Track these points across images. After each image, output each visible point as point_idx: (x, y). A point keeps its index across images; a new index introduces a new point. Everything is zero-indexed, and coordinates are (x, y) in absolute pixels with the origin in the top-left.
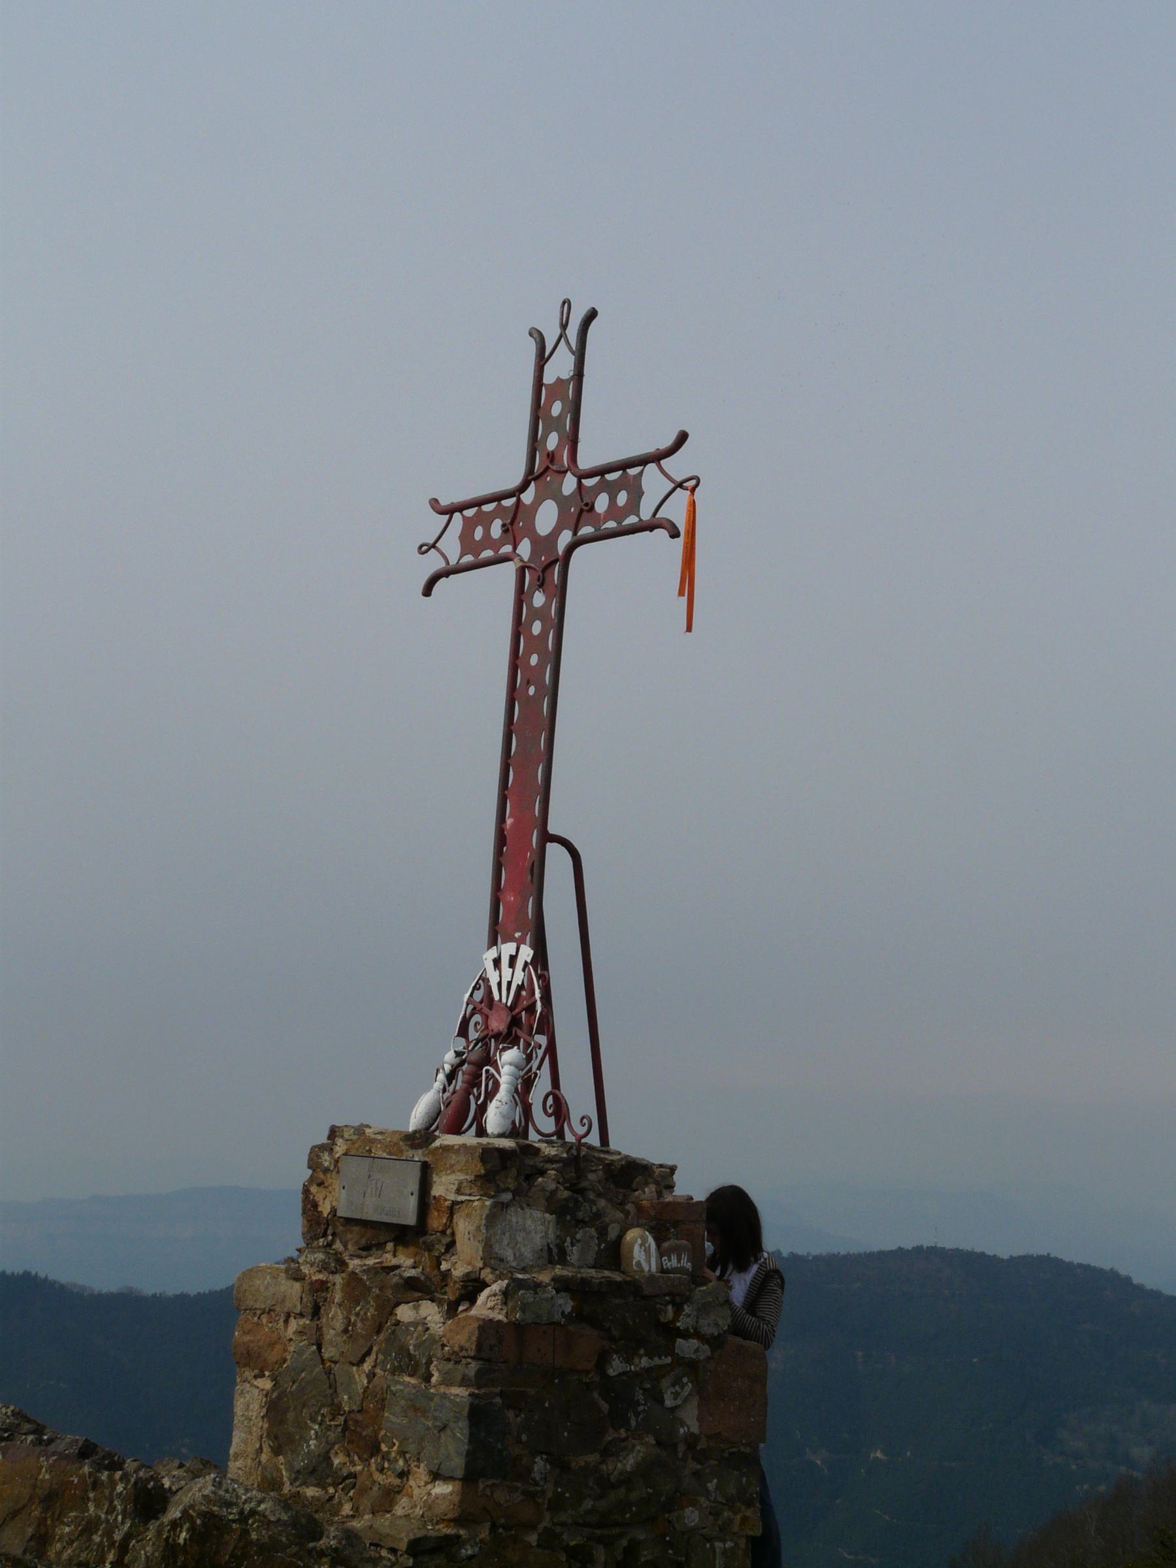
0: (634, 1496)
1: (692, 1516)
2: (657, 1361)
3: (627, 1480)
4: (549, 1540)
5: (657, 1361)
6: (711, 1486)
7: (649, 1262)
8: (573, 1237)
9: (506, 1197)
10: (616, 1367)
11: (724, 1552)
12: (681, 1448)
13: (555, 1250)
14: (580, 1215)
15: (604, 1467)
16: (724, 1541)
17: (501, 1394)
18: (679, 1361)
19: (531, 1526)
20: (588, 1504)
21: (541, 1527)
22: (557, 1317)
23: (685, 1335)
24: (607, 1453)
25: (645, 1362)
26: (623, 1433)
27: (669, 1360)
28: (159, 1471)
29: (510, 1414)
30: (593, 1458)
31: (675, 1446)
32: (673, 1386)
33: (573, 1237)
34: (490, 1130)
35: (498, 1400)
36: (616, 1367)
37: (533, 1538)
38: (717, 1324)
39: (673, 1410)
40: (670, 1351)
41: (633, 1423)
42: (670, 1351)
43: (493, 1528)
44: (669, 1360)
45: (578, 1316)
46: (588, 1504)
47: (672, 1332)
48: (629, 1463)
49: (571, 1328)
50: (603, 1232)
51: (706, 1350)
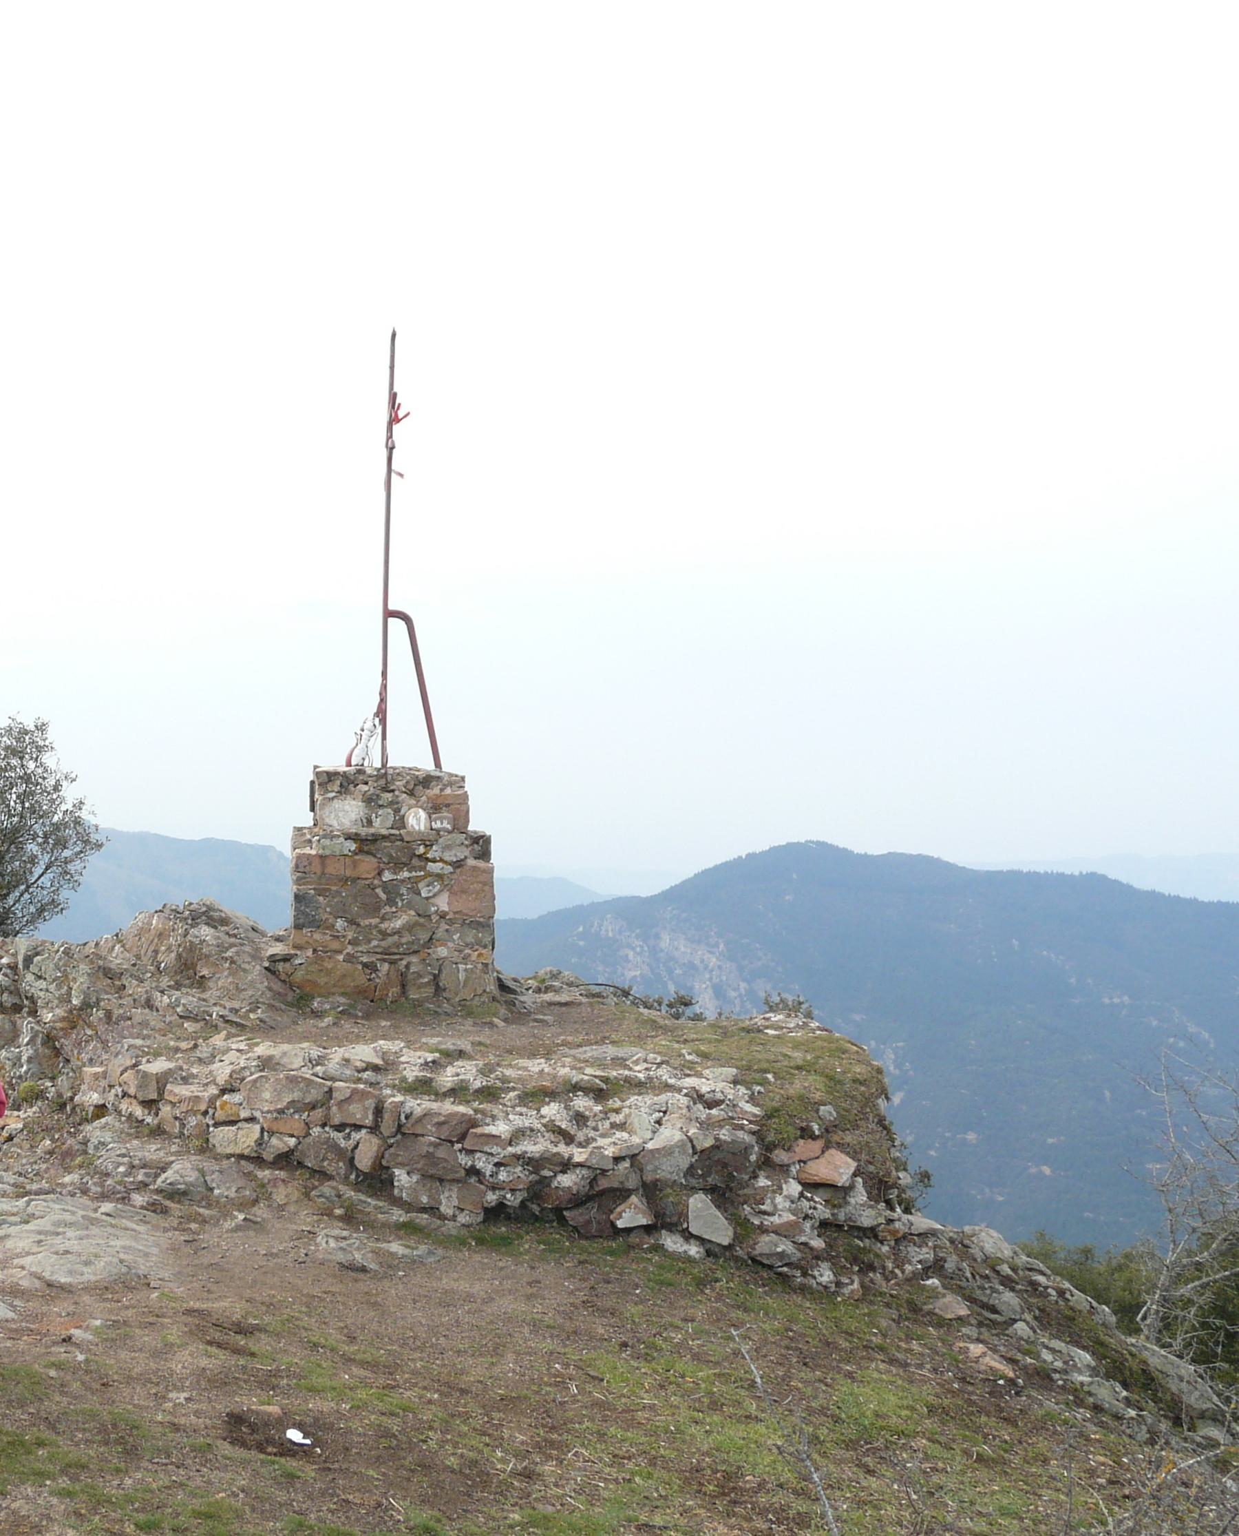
0: (404, 940)
1: (442, 952)
2: (414, 874)
3: (398, 932)
4: (350, 958)
5: (414, 874)
6: (455, 937)
7: (419, 825)
8: (376, 814)
9: (331, 795)
10: (387, 876)
11: (466, 970)
12: (435, 918)
13: (365, 821)
14: (381, 803)
15: (382, 925)
16: (466, 964)
17: (314, 889)
18: (430, 874)
19: (340, 952)
20: (375, 943)
21: (345, 952)
22: (346, 852)
23: (434, 861)
24: (383, 919)
25: (406, 874)
26: (394, 909)
27: (422, 873)
28: (688, 984)
29: (321, 899)
30: (374, 921)
31: (429, 916)
32: (428, 886)
33: (376, 814)
34: (353, 763)
35: (312, 892)
36: (387, 876)
37: (341, 957)
38: (456, 855)
39: (427, 898)
40: (423, 868)
41: (400, 904)
42: (423, 868)
43: (315, 951)
44: (422, 873)
45: (360, 851)
46: (375, 943)
47: (424, 858)
48: (398, 924)
49: (357, 857)
50: (397, 811)
51: (450, 869)
